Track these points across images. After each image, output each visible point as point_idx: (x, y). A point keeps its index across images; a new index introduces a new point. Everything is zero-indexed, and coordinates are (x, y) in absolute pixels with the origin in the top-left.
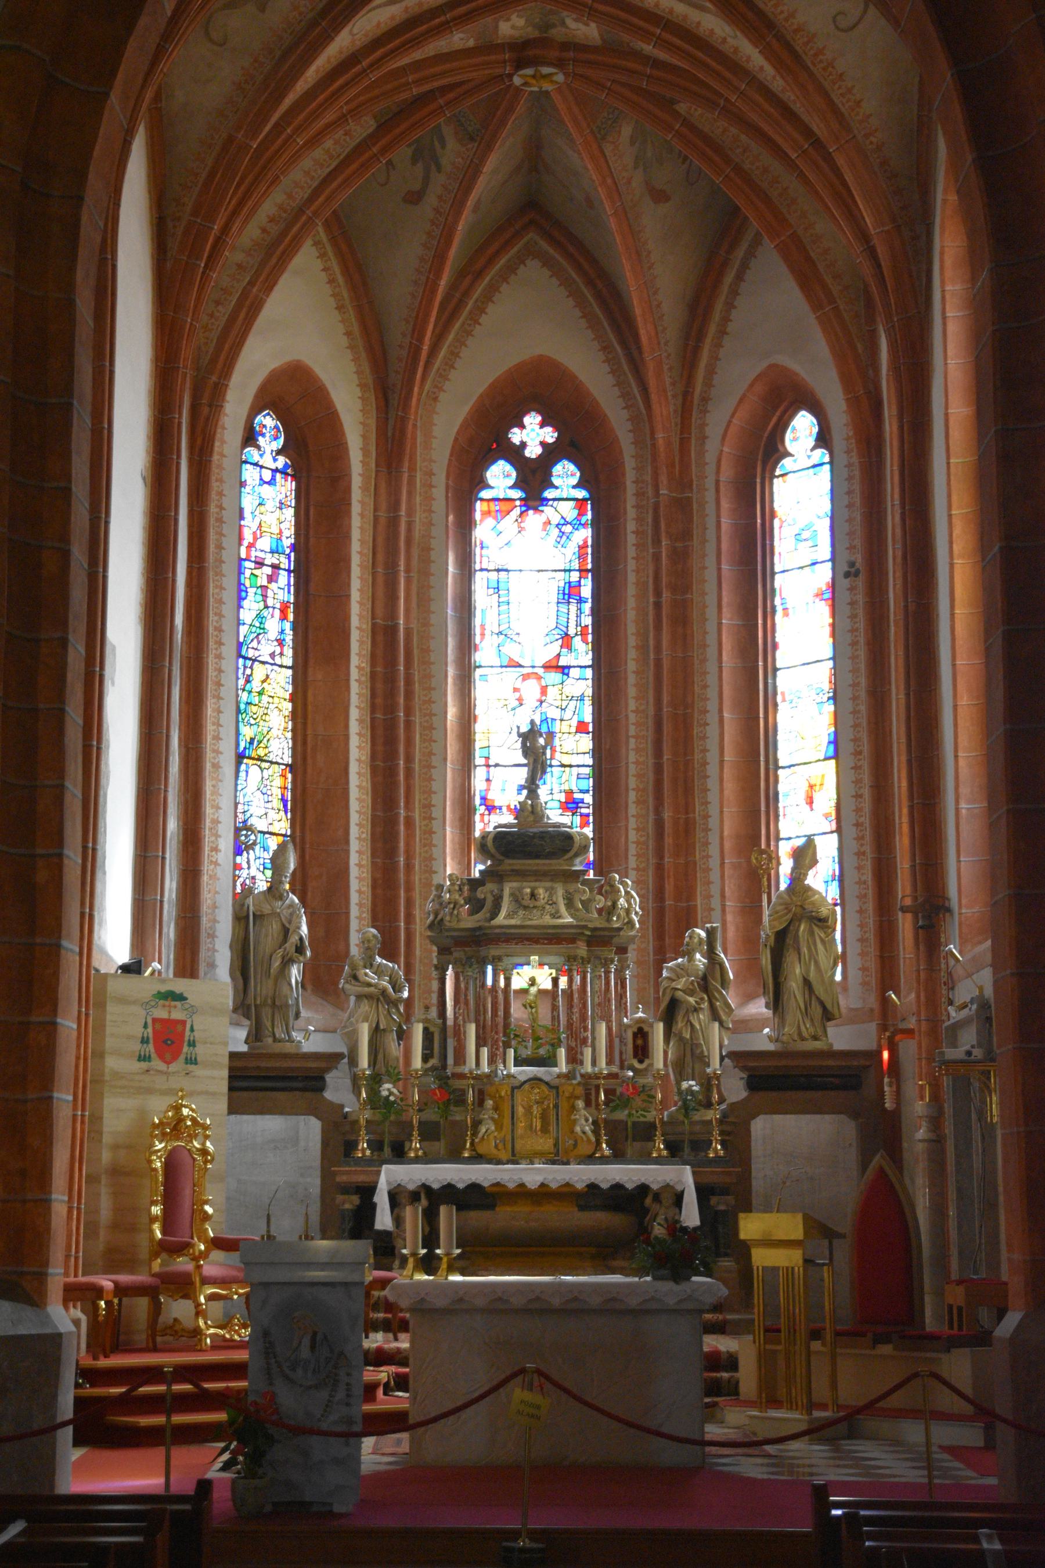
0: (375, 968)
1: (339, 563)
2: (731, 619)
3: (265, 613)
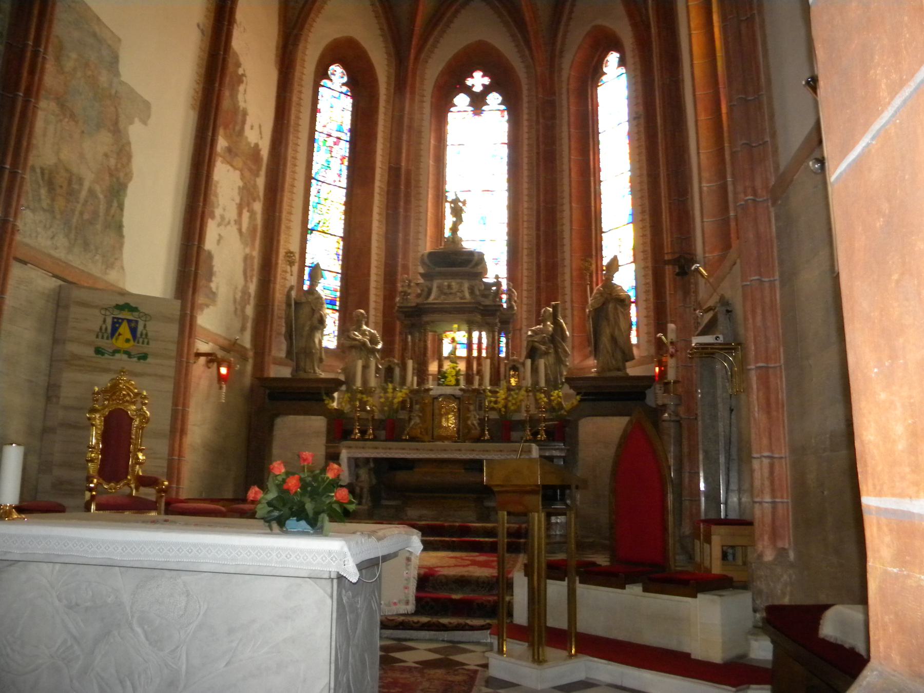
3: (330, 159)
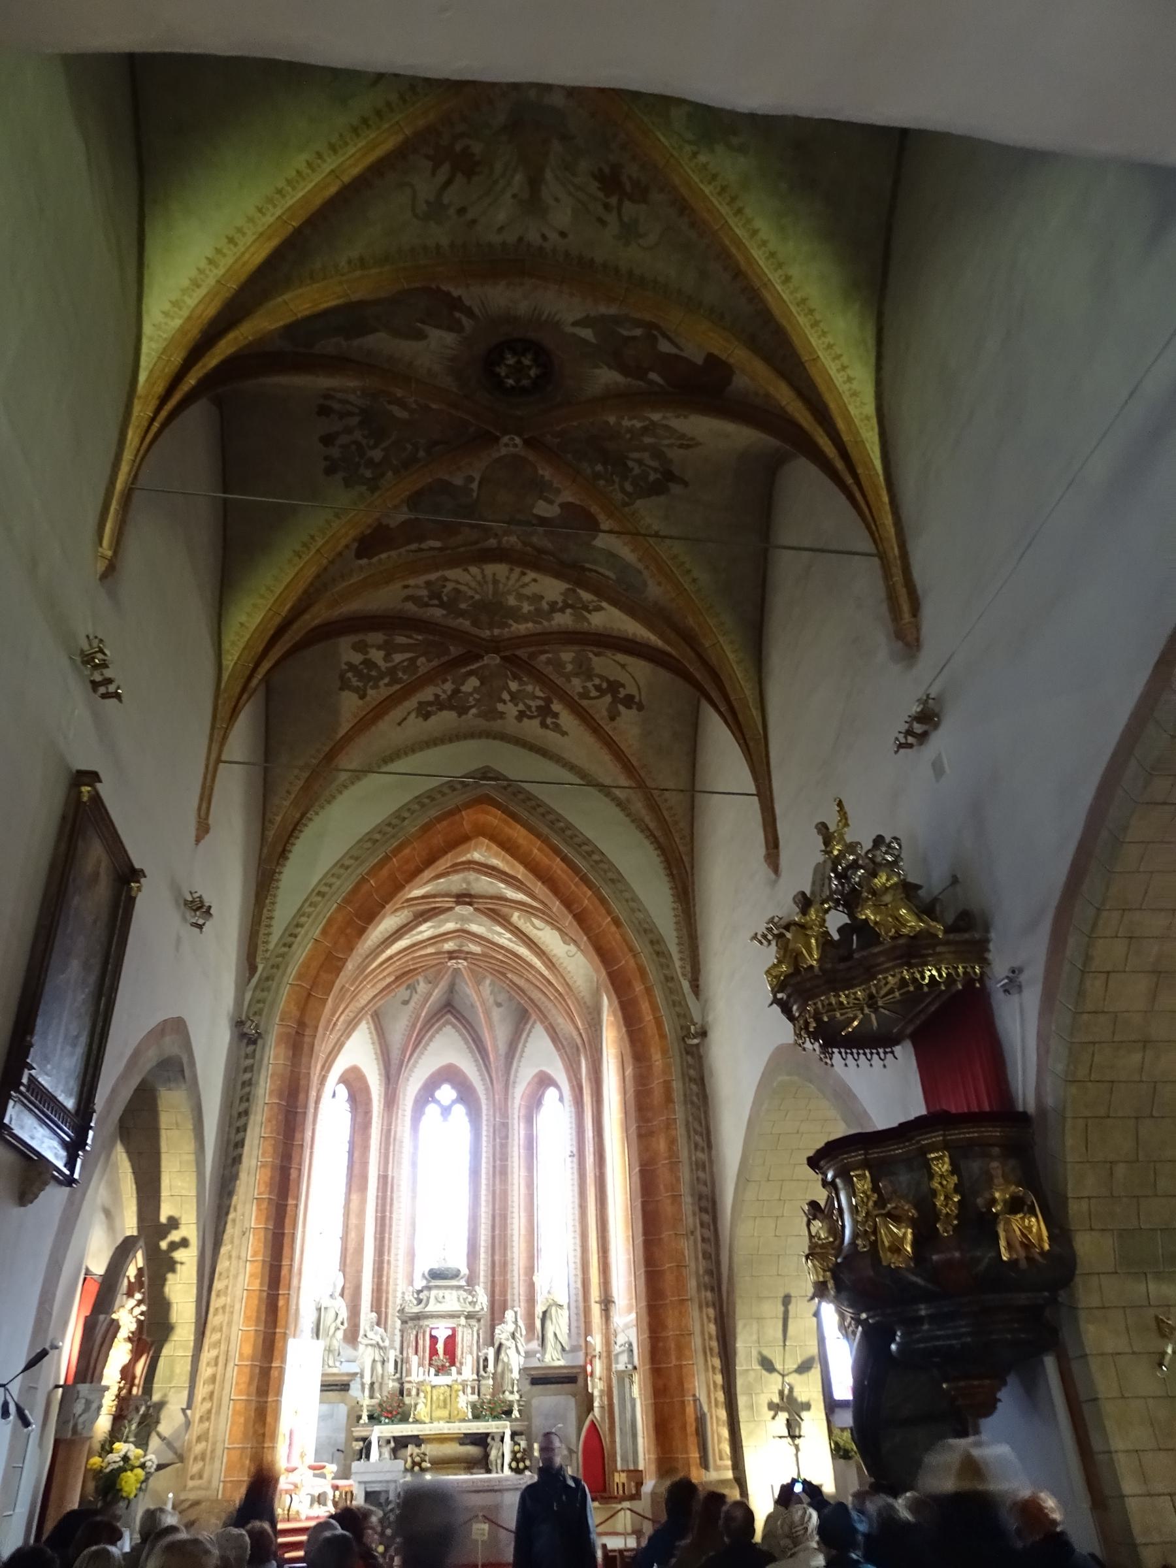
1: (366, 1148)
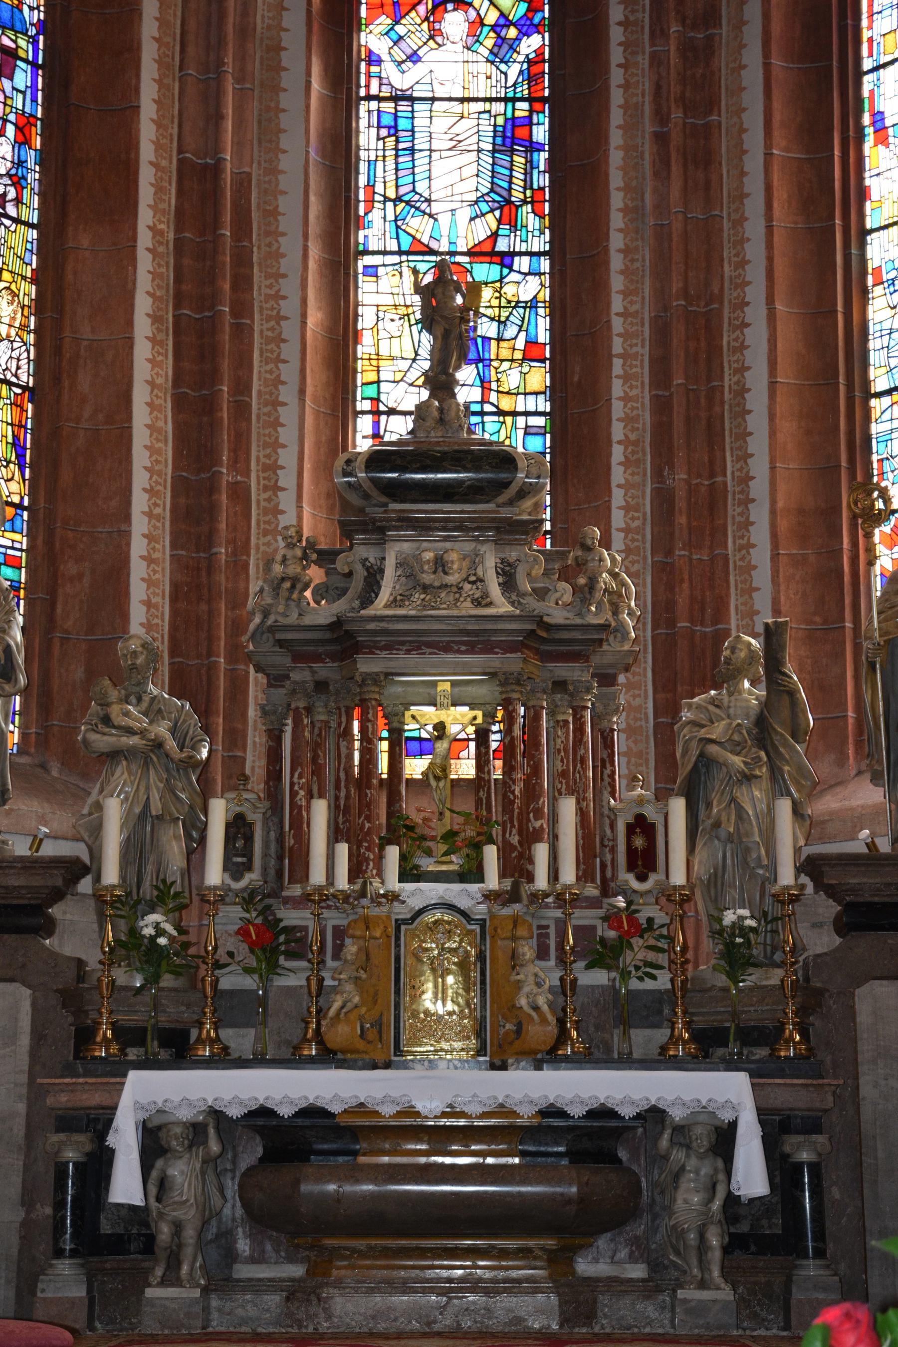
0: (144, 705)
2: (787, 149)
